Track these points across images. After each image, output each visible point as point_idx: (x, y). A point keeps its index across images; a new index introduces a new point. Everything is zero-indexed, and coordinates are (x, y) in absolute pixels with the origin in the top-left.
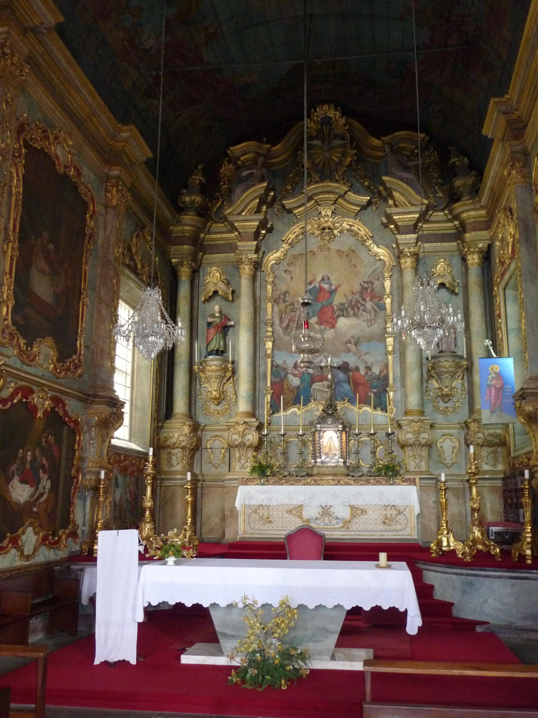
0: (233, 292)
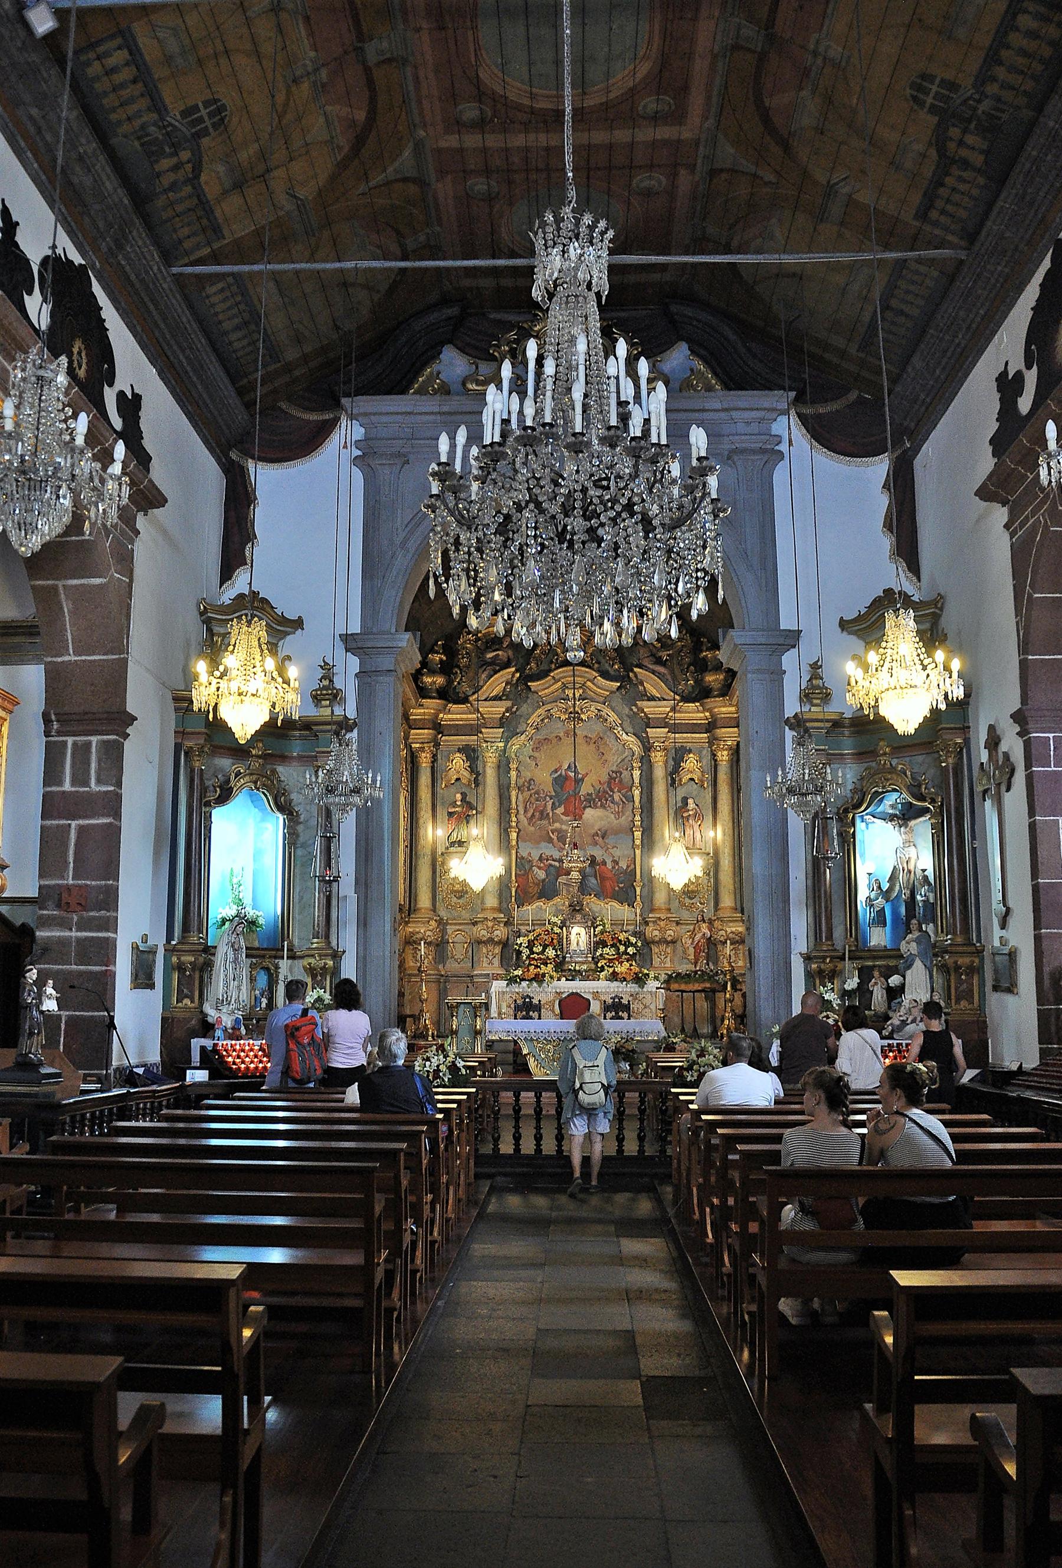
0: (476, 780)
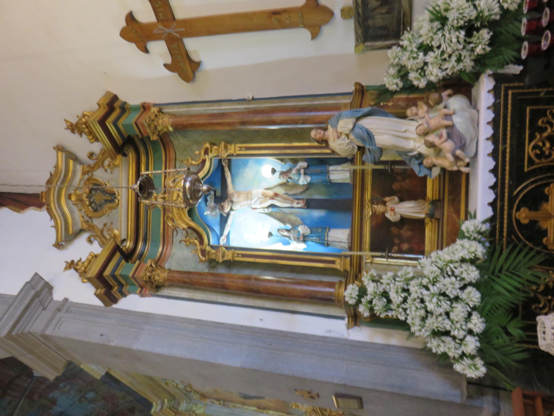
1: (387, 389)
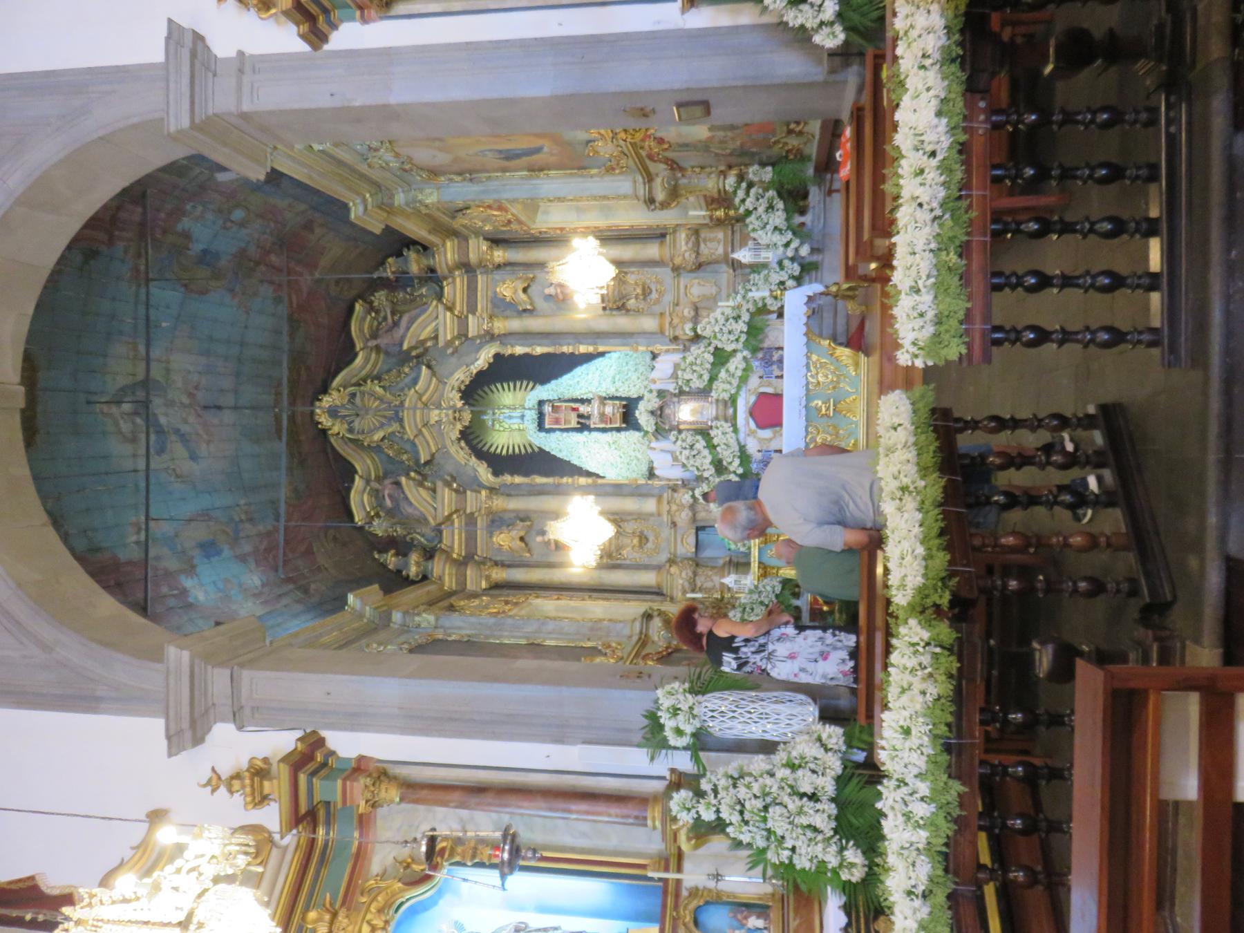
0: (522, 520)
1: (740, 83)
